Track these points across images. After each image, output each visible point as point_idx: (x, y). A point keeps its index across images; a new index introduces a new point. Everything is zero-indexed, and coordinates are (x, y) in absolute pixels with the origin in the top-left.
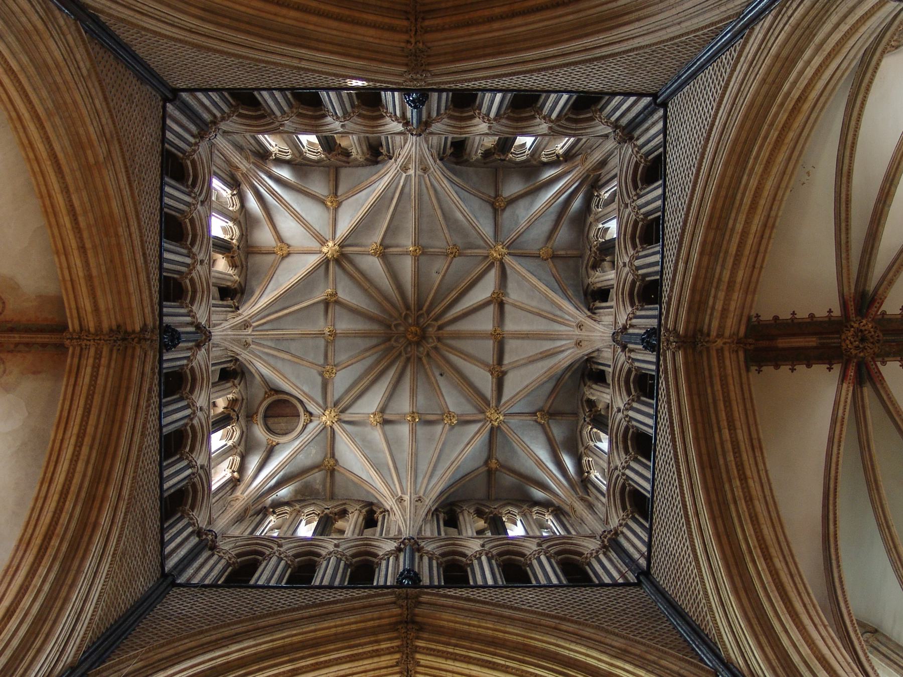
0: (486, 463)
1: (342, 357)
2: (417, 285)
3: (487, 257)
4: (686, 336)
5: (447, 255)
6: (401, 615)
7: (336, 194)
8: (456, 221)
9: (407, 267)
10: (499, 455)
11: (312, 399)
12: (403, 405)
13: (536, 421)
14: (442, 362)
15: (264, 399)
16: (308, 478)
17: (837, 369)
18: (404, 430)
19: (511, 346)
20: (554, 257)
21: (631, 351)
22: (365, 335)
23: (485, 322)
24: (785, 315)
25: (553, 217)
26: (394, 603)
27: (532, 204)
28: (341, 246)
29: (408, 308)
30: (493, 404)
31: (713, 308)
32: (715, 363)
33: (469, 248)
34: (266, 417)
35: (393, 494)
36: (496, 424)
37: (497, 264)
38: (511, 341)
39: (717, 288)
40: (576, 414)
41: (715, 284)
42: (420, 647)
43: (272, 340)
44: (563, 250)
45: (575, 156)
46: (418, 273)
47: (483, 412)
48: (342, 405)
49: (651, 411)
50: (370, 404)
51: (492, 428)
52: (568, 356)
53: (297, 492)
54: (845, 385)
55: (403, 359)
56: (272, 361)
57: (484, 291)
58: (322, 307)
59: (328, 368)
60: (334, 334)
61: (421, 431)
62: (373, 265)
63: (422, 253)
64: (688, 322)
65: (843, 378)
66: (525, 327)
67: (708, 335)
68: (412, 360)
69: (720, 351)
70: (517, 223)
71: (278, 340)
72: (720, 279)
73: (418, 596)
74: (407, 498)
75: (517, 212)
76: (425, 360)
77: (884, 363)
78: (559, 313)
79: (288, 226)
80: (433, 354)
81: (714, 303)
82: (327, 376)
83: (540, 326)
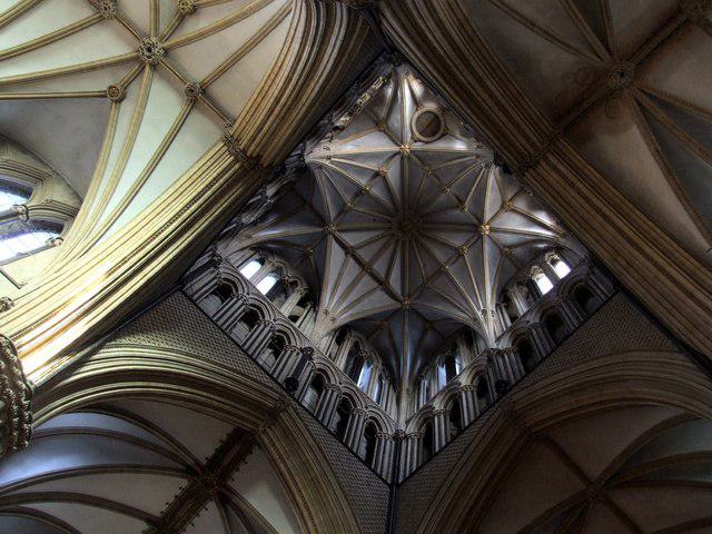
2: (428, 251)
7: (507, 256)
18: (363, 181)
20: (379, 327)
21: (298, 354)
28: (481, 237)
30: (337, 234)
37: (402, 298)
50: (392, 172)
53: (384, 96)
57: (395, 282)
60: (444, 191)
62: (456, 241)
63: (441, 271)
65: (197, 463)
79: (514, 223)
80: (388, 225)
82: (427, 168)
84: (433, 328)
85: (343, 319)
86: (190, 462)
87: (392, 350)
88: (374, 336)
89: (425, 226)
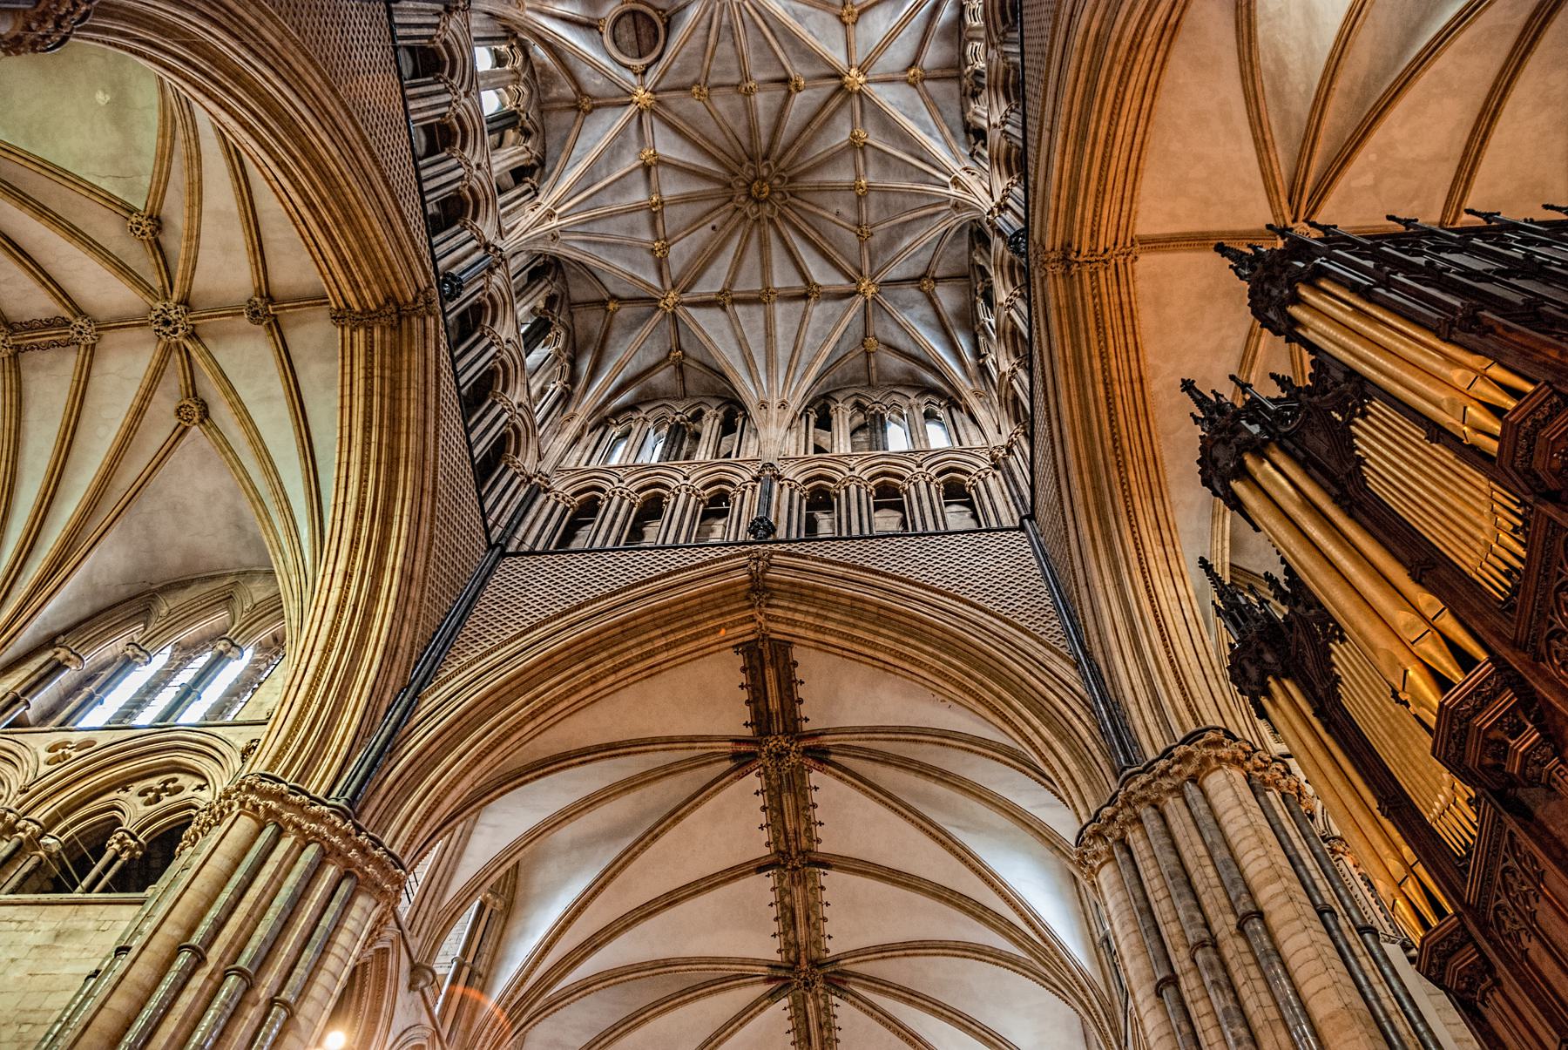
0: (614, 297)
1: (721, 105)
2: (821, 189)
3: (861, 274)
4: (765, 580)
5: (859, 226)
6: (406, 302)
8: (901, 238)
9: (842, 175)
10: (625, 312)
11: (664, 73)
12: (672, 188)
13: (671, 351)
14: (729, 227)
15: (656, 10)
16: (563, 79)
17: (748, 732)
18: (640, 195)
19: (758, 312)
22: (752, 130)
23: (783, 278)
24: (799, 673)
25: (914, 350)
26: (418, 289)
27: (927, 324)
29: (792, 179)
30: (685, 297)
31: (796, 610)
32: (737, 616)
33: (870, 253)
34: (633, 13)
35: (557, 205)
36: (661, 305)
37: (853, 287)
38: (762, 313)
39: (817, 615)
40: (685, 395)
41: (821, 612)
42: (372, 333)
43: (730, 22)
44: (877, 364)
45: (982, 374)
46: (835, 189)
47: (674, 286)
48: (661, 110)
49: (681, 541)
50: (667, 146)
51: (656, 300)
52: (749, 392)
54: (730, 744)
55: (729, 178)
56: (704, 24)
58: (781, 75)
59: (705, 91)
60: (749, 93)
61: (642, 218)
63: (860, 196)
64: (780, 582)
65: (737, 741)
66: (780, 330)
67: (768, 606)
68: (729, 190)
69: (752, 619)
70: (904, 308)
71: (732, 28)
72: (826, 618)
73: (431, 314)
74: (555, 222)
75: (917, 306)
76: (730, 206)
77: (759, 775)
78: (799, 373)
80: (739, 215)
81: (801, 612)
82: (695, 89)
83: (783, 350)
84: (935, 280)
85: (799, 392)
86: (728, 747)
87: (913, 365)
88: (874, 372)
89: (782, 164)
